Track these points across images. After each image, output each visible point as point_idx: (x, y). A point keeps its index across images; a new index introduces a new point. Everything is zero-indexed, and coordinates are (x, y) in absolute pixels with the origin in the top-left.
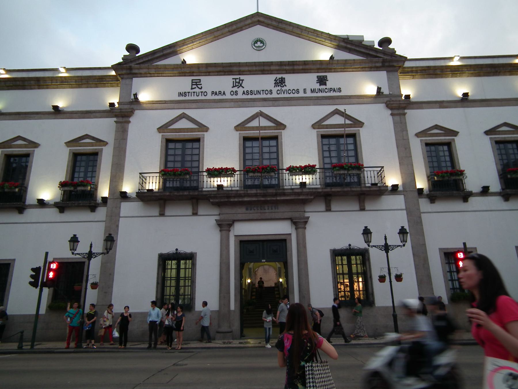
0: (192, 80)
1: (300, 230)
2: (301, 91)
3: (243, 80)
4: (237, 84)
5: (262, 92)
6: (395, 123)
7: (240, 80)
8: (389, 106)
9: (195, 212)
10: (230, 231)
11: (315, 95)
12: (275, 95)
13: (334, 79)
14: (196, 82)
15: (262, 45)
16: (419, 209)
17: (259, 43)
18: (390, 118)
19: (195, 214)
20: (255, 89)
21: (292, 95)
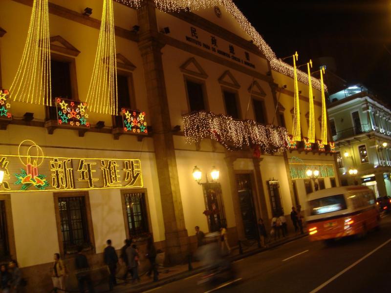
12: (230, 59)
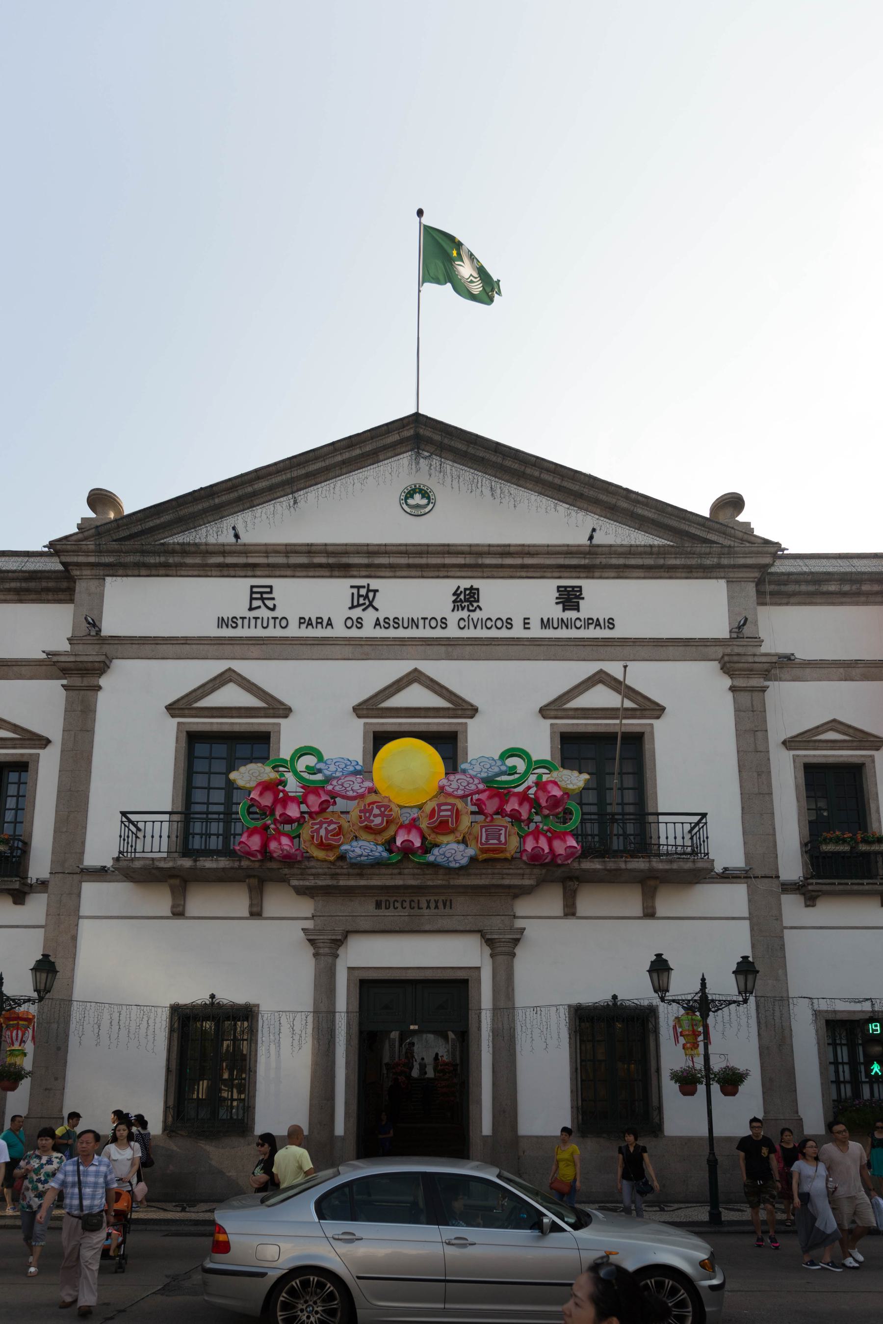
0: (252, 587)
1: (500, 959)
2: (518, 623)
3: (376, 591)
4: (361, 601)
5: (421, 623)
6: (737, 710)
7: (369, 591)
8: (728, 668)
9: (255, 909)
10: (337, 956)
11: (549, 633)
12: (453, 631)
13: (601, 596)
14: (261, 593)
15: (425, 501)
16: (779, 918)
17: (417, 497)
18: (730, 695)
19: (256, 914)
20: (404, 614)
21: (494, 633)
